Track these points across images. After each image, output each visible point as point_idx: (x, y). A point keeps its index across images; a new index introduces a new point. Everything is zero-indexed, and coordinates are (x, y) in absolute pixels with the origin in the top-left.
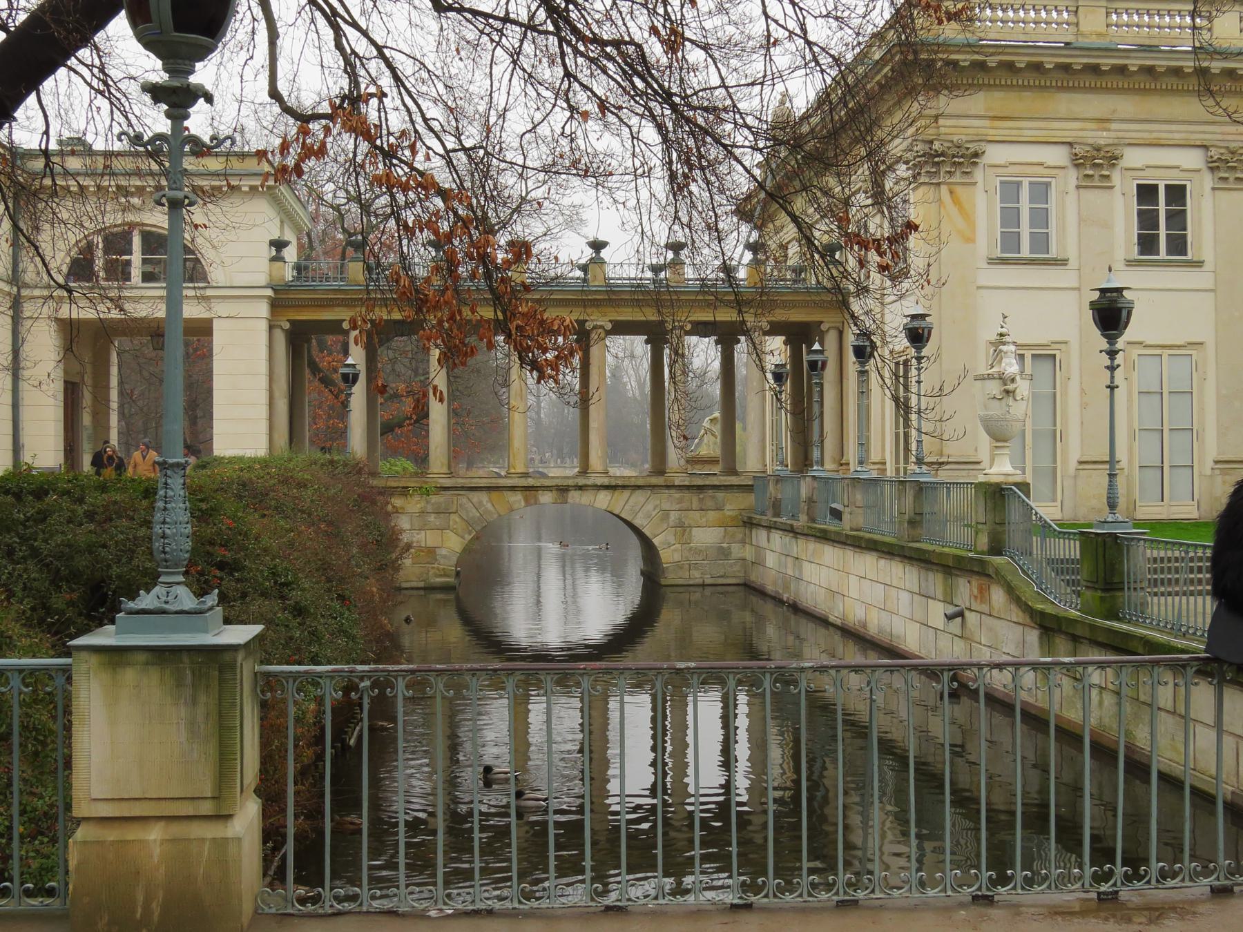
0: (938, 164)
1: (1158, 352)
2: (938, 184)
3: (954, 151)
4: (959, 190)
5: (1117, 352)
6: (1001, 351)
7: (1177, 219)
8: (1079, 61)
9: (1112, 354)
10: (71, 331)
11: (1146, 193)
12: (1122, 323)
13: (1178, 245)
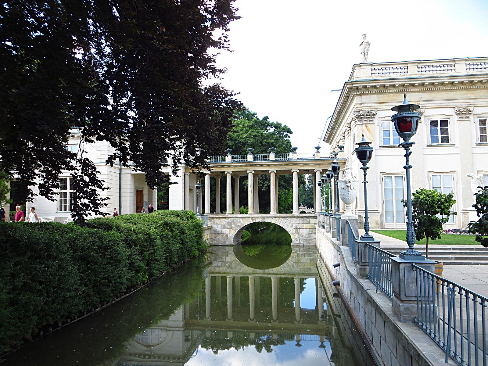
2: (362, 124)
4: (368, 126)
7: (445, 132)
8: (407, 83)
9: (365, 169)
11: (433, 123)
12: (367, 157)
13: (445, 139)
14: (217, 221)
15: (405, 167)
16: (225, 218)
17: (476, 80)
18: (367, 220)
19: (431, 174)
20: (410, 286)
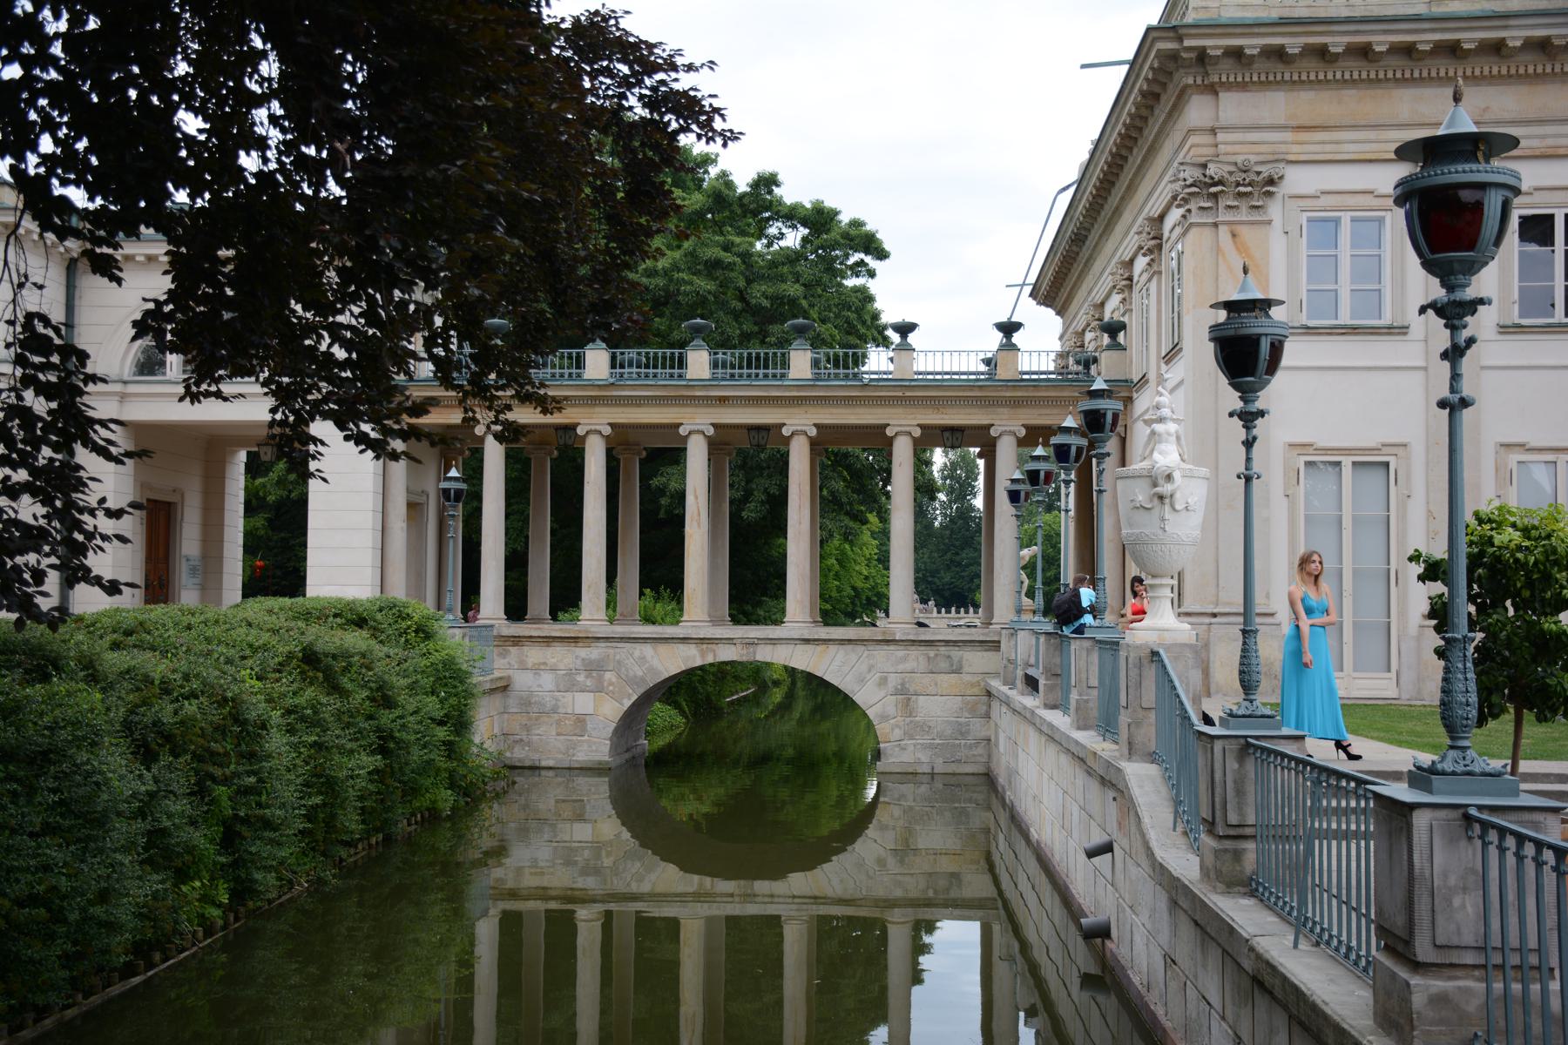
0: (1215, 196)
1: (1550, 457)
2: (1216, 225)
3: (1239, 177)
4: (1244, 231)
6: (1153, 433)
8: (1426, 39)
9: (1248, 418)
12: (1263, 364)
14: (534, 654)
15: (1442, 404)
16: (575, 640)
18: (1251, 641)
19: (1515, 457)
20: (1457, 902)
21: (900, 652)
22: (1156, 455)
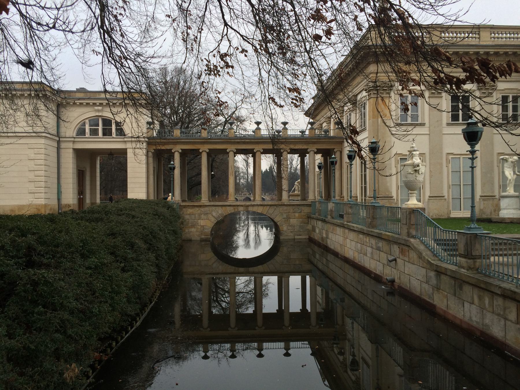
5: (475, 151)
6: (412, 154)
10: (79, 153)
12: (478, 138)
14: (190, 211)
16: (200, 206)
17: (501, 51)
19: (451, 157)
21: (285, 208)
22: (414, 160)
